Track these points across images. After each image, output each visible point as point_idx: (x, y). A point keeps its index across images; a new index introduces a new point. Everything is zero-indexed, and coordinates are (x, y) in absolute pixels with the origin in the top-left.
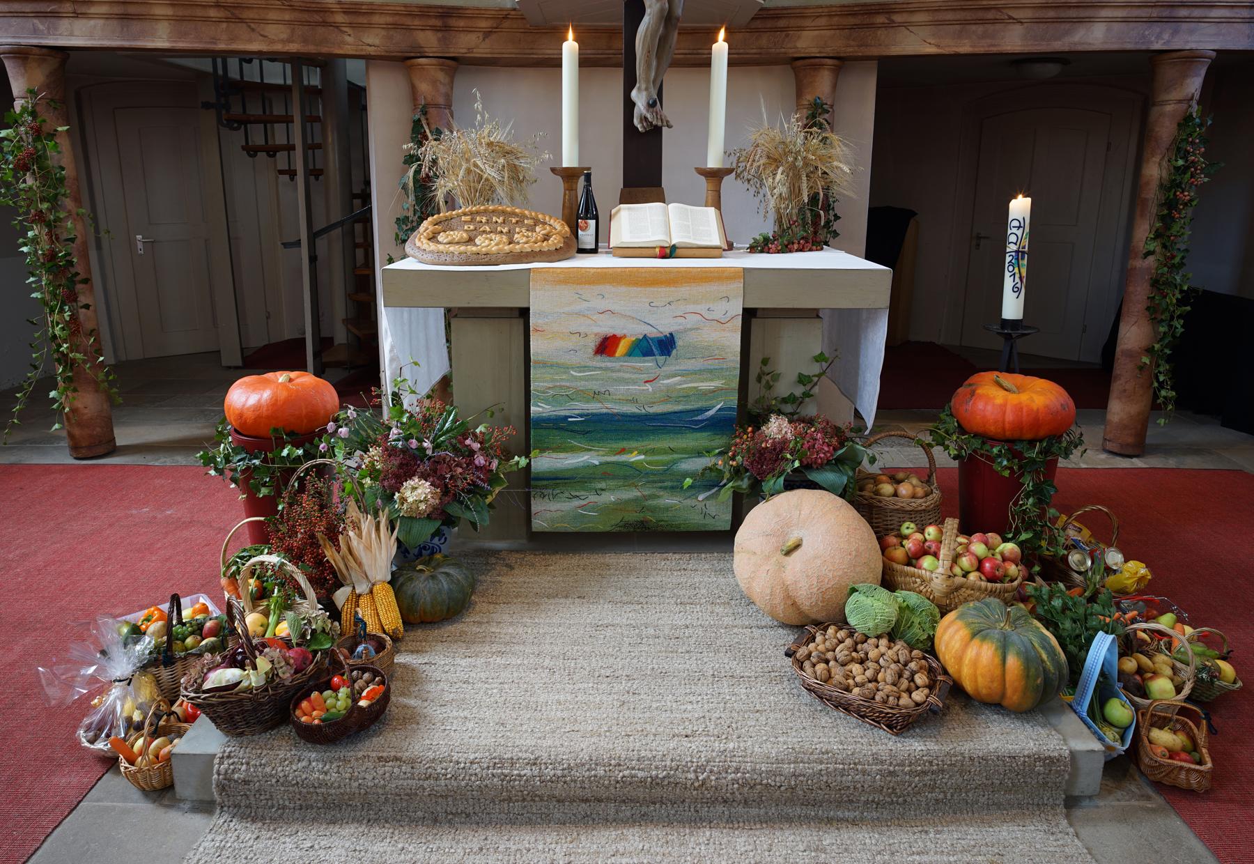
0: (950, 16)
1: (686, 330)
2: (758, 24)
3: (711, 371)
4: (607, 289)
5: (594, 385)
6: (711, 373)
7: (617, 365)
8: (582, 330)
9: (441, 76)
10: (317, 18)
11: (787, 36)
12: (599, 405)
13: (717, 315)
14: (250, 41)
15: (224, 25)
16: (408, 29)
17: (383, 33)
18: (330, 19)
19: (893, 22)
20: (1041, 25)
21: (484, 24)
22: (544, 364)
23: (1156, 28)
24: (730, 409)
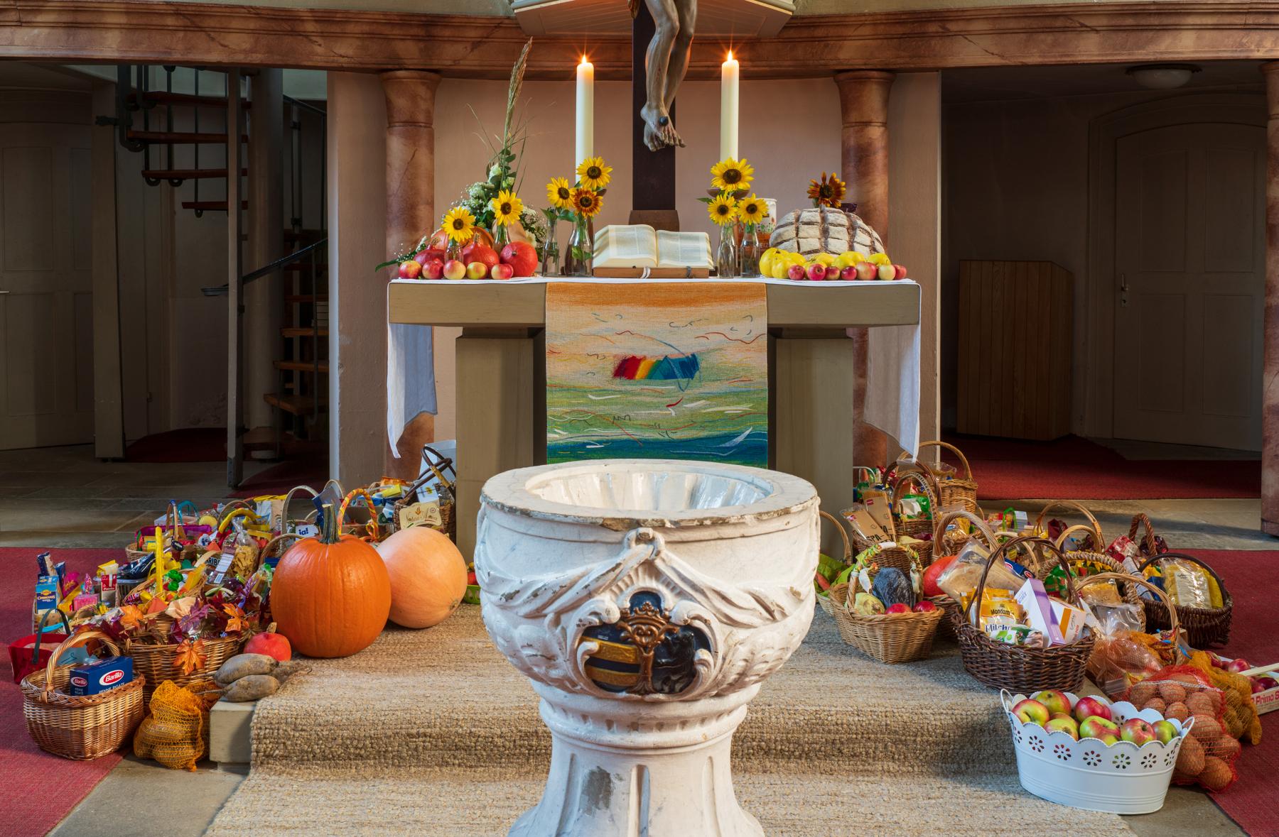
0: (1012, 24)
1: (709, 351)
2: (792, 33)
3: (736, 394)
5: (615, 410)
6: (737, 396)
7: (637, 388)
8: (600, 351)
9: (422, 91)
10: (286, 26)
11: (826, 46)
12: (620, 431)
13: (741, 335)
14: (209, 51)
15: (181, 34)
16: (387, 39)
17: (359, 43)
18: (301, 29)
19: (949, 30)
20: (1120, 34)
21: (472, 33)
22: (562, 388)
23: (1255, 36)
24: (760, 435)
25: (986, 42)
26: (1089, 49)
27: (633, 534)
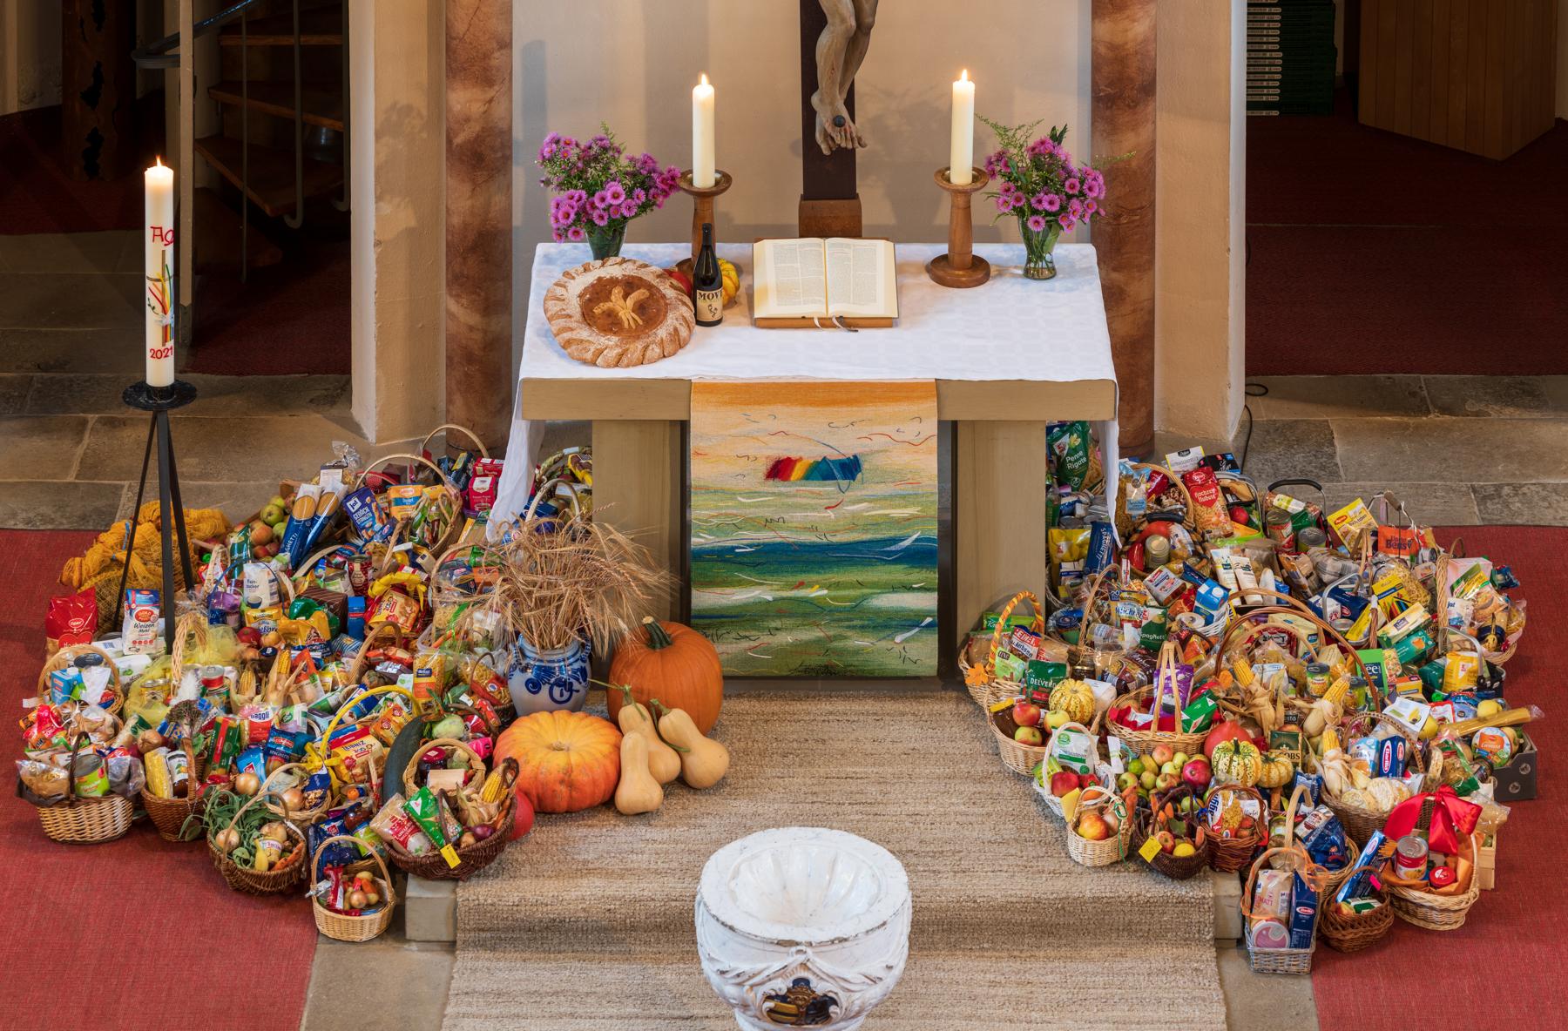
1: (873, 453)
3: (903, 497)
5: (767, 513)
6: (905, 499)
7: (792, 489)
8: (751, 453)
12: (772, 534)
22: (707, 490)
24: (929, 540)
27: (794, 949)
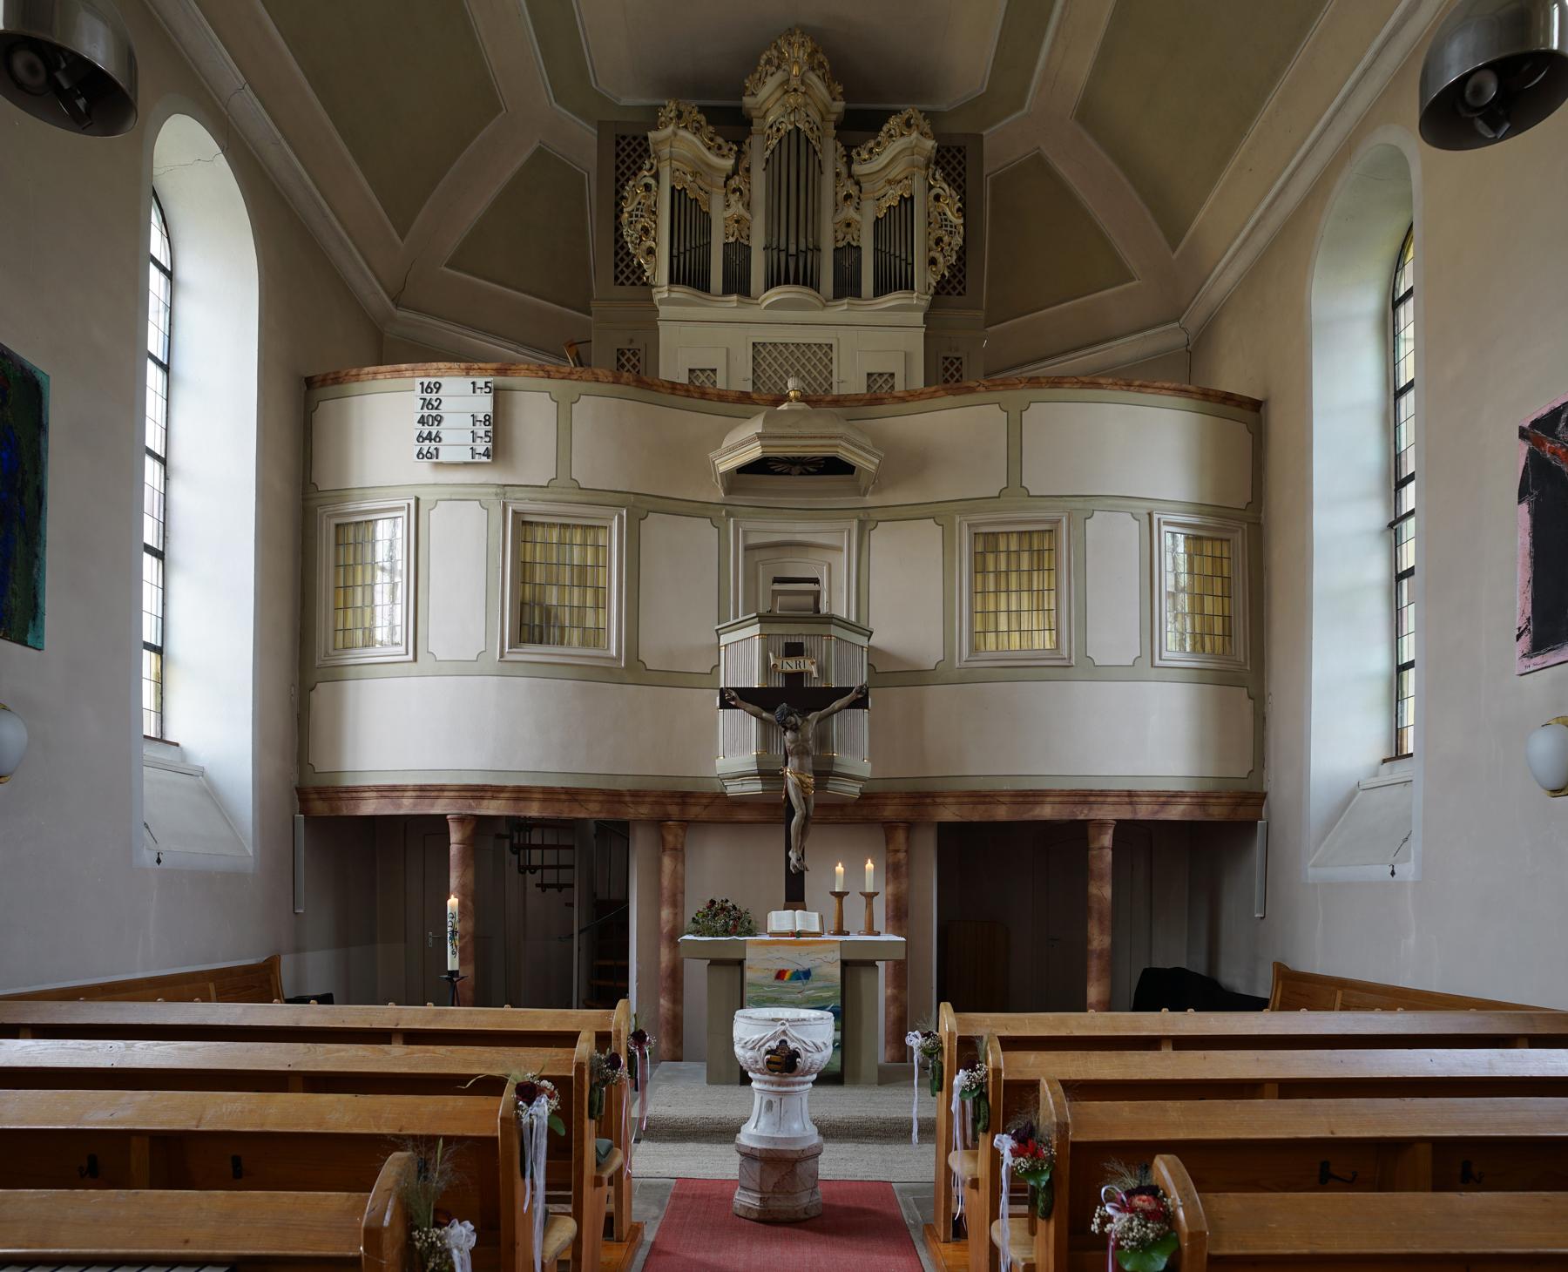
4: (780, 947)
6: (827, 988)
25: (954, 808)
26: (1002, 813)
